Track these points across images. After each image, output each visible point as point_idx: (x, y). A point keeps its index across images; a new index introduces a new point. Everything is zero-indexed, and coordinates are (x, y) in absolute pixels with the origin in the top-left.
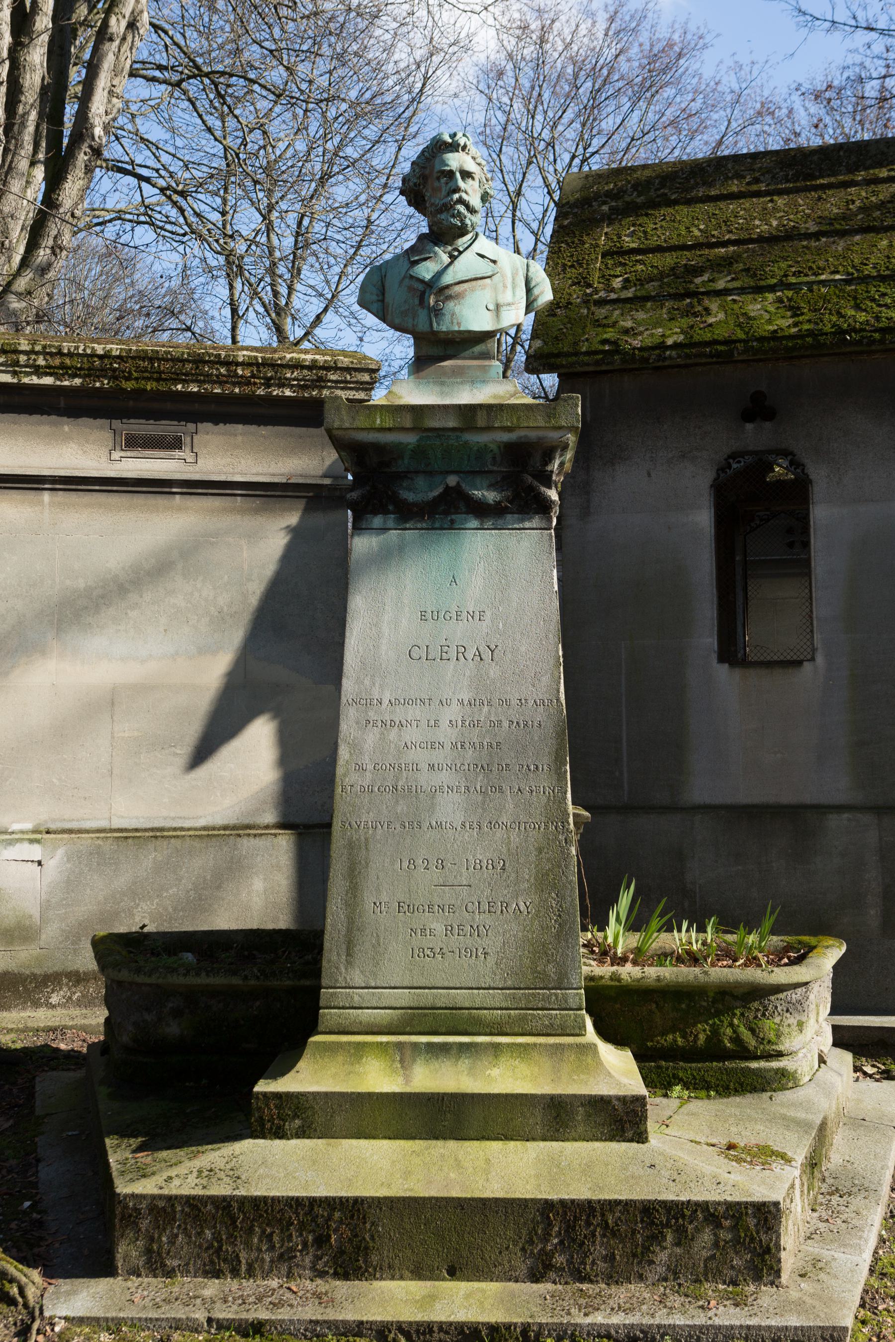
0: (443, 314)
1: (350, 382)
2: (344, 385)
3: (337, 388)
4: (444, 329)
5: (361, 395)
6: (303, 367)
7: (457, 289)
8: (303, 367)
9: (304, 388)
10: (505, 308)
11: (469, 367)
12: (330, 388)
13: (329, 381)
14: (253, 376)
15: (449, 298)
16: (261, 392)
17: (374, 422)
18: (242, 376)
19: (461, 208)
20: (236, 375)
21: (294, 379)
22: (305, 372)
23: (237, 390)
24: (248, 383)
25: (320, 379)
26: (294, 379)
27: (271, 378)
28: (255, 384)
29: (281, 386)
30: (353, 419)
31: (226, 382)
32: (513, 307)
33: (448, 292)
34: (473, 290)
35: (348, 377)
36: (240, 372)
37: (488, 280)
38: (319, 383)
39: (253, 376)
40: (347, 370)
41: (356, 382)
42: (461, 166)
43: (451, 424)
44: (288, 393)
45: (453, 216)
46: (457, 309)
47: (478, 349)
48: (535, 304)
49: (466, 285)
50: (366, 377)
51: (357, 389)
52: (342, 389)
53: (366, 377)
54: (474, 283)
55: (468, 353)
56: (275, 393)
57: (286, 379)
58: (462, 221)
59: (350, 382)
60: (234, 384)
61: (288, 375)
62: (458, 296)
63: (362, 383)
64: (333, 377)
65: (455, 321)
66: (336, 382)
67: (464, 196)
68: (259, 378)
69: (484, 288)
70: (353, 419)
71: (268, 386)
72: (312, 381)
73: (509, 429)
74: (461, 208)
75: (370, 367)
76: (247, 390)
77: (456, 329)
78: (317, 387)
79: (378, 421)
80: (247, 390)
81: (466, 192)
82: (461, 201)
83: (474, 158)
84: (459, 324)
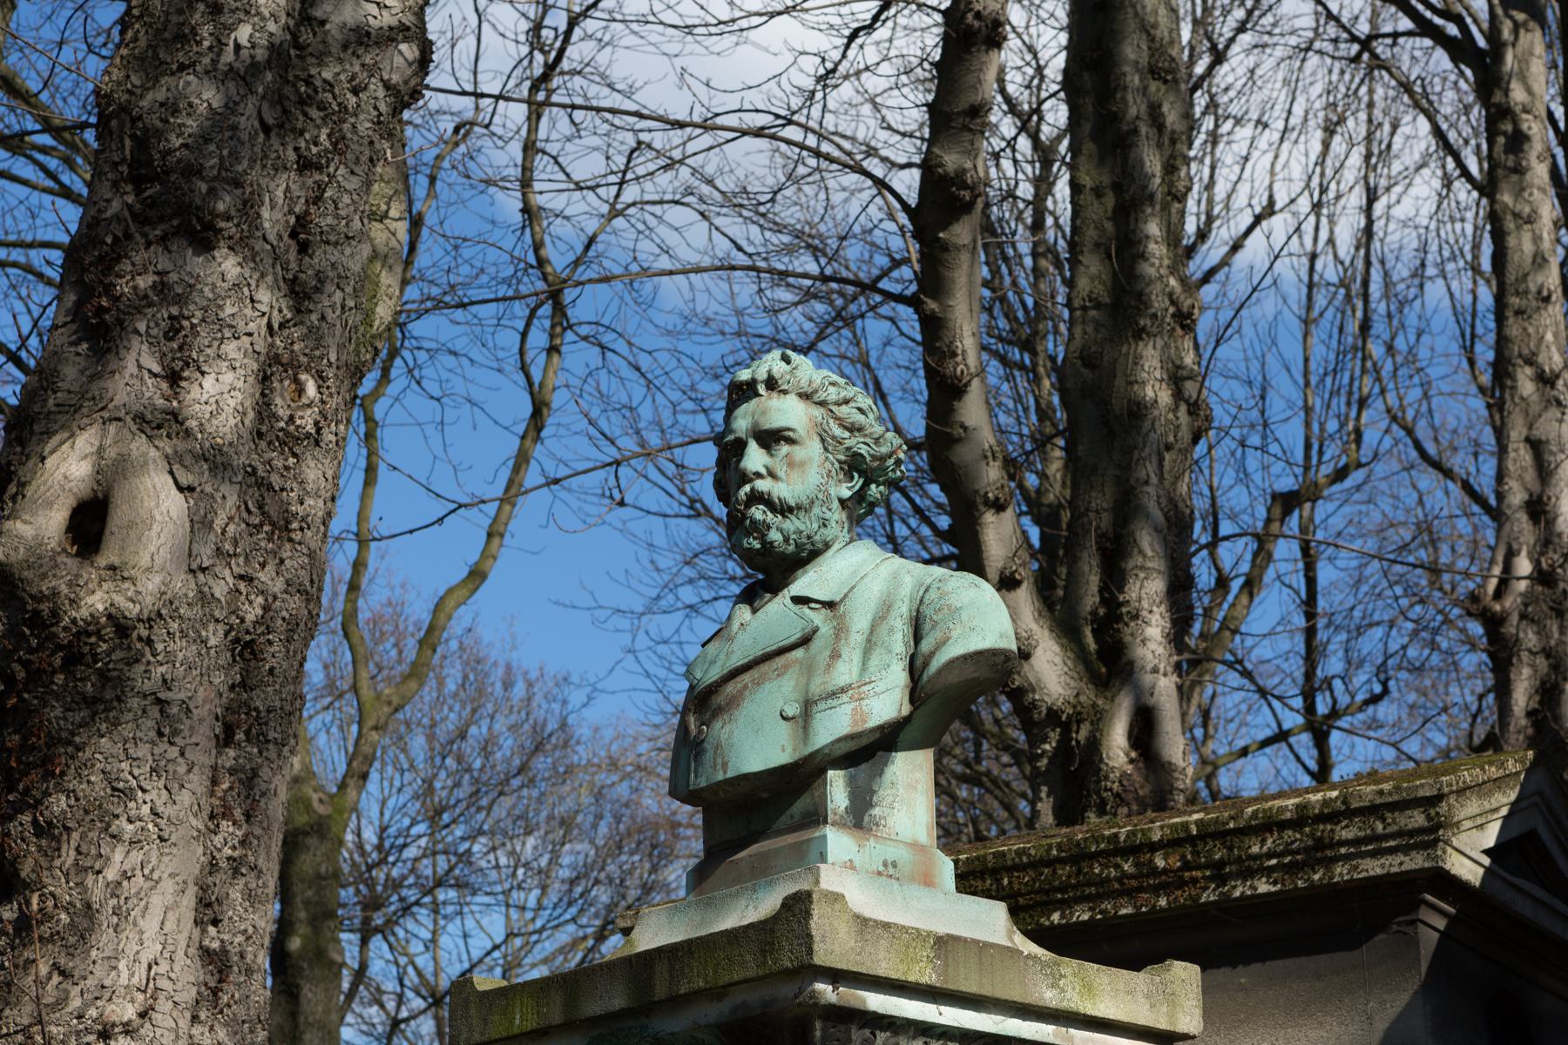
0: (704, 750)
1: (1386, 837)
2: (1374, 845)
3: (1363, 855)
4: (703, 784)
5: (1416, 862)
6: (1283, 825)
7: (731, 688)
8: (1283, 825)
9: (1293, 869)
10: (822, 705)
11: (776, 852)
12: (1347, 858)
13: (1342, 843)
14: (1187, 866)
15: (718, 711)
16: (1209, 896)
17: (512, 1023)
18: (1165, 871)
19: (758, 513)
20: (1154, 872)
21: (1270, 855)
22: (1289, 834)
23: (1163, 902)
24: (1181, 884)
25: (1320, 844)
26: (1270, 855)
27: (1221, 864)
28: (1194, 881)
29: (1248, 874)
30: (485, 1021)
31: (1140, 889)
32: (845, 698)
33: (719, 699)
34: (758, 683)
35: (1379, 827)
36: (1160, 863)
37: (799, 653)
38: (1321, 852)
39: (1187, 866)
40: (1374, 810)
41: (1393, 836)
42: (755, 425)
43: (618, 1002)
44: (1263, 887)
45: (748, 534)
46: (724, 736)
47: (799, 807)
48: (925, 677)
49: (746, 677)
50: (1418, 819)
51: (1405, 850)
52: (1374, 854)
53: (1418, 819)
54: (764, 667)
55: (784, 820)
56: (1237, 894)
57: (1255, 858)
58: (763, 538)
59: (1386, 837)
60: (1156, 890)
61: (1255, 849)
62: (734, 702)
63: (1412, 833)
64: (1347, 834)
65: (719, 761)
66: (1356, 842)
67: (763, 485)
68: (1199, 867)
69: (786, 667)
70: (485, 1021)
71: (1221, 880)
72: (1307, 850)
73: (717, 993)
74: (758, 513)
75: (1421, 793)
76: (1182, 896)
77: (720, 777)
78: (1320, 862)
79: (517, 1022)
80: (1182, 896)
81: (772, 474)
82: (757, 498)
83: (805, 396)
84: (725, 765)
